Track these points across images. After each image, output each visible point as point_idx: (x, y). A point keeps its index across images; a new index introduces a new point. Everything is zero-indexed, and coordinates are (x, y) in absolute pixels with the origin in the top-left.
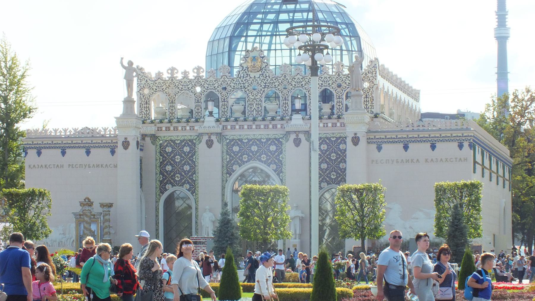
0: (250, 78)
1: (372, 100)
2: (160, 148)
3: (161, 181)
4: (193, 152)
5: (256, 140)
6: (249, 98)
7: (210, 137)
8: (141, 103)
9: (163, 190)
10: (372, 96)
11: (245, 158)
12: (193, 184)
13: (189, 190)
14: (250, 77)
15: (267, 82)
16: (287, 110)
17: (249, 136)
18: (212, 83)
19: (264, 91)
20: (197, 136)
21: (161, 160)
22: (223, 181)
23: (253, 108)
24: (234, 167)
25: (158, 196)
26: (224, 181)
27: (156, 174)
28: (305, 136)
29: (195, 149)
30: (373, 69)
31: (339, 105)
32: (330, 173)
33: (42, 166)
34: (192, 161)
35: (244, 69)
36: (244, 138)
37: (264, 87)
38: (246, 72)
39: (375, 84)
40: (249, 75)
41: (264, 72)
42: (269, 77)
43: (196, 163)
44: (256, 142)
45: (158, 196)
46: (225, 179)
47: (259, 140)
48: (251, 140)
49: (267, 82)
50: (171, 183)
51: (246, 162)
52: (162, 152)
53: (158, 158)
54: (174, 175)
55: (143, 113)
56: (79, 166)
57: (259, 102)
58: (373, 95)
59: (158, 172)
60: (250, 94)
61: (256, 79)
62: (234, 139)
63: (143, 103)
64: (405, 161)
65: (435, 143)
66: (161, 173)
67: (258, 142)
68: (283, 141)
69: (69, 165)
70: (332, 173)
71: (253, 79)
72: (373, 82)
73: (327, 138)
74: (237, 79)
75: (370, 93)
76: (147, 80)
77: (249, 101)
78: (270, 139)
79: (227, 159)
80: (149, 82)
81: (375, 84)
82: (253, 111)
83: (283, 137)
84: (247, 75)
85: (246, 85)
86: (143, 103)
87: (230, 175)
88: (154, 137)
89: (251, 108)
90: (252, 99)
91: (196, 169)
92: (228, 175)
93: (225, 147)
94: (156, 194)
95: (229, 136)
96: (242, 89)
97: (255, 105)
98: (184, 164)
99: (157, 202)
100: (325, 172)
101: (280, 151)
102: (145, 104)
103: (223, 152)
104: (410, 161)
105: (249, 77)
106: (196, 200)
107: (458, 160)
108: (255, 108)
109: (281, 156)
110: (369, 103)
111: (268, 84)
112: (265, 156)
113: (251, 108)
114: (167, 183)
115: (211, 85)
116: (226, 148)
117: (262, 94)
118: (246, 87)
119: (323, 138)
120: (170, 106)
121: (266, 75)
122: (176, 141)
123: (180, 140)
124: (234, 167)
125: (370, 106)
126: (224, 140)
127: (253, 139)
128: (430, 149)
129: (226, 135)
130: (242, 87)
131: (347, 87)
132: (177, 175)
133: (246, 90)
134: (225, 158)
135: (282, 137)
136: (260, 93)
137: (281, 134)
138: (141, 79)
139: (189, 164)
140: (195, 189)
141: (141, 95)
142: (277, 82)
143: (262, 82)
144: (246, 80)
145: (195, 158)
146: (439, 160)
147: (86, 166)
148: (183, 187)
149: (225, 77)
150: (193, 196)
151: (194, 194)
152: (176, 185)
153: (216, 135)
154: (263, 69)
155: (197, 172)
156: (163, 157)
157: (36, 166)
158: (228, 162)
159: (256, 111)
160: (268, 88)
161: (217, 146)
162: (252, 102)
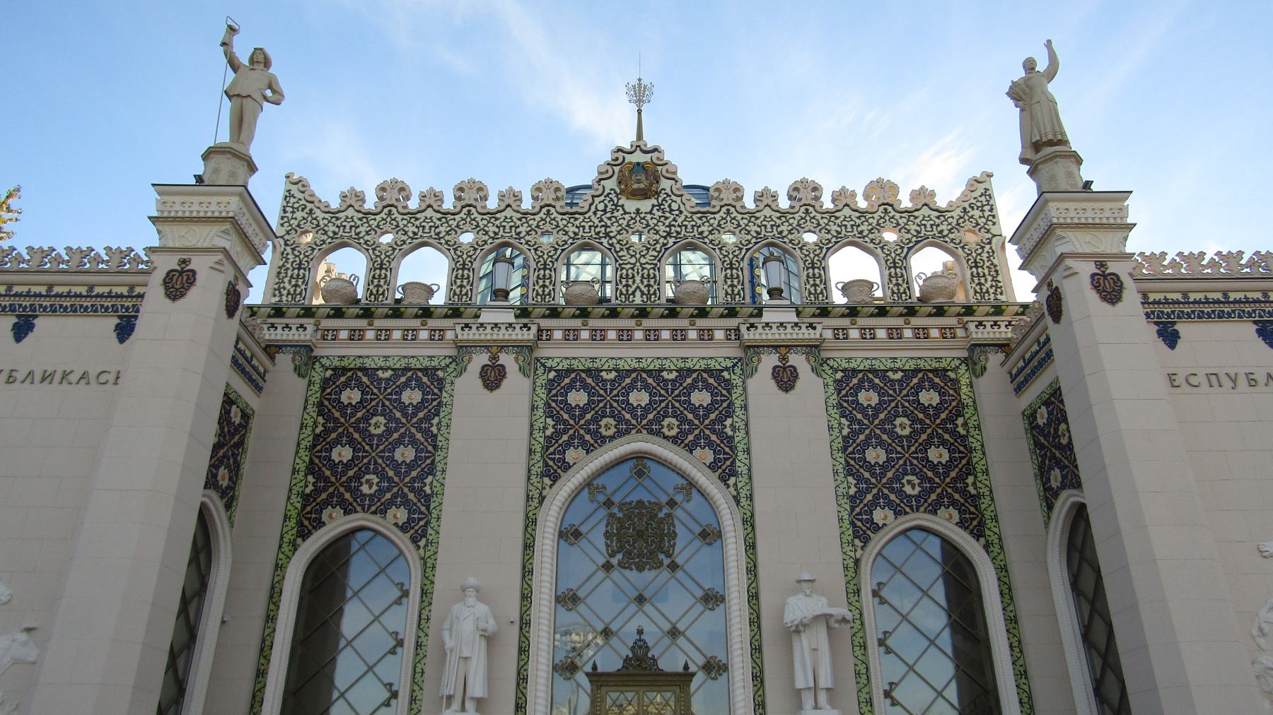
0: (626, 213)
2: (323, 392)
4: (433, 405)
5: (644, 375)
6: (621, 262)
7: (494, 358)
8: (283, 265)
9: (307, 524)
10: (992, 264)
11: (607, 427)
12: (423, 509)
13: (403, 528)
14: (623, 209)
15: (673, 223)
20: (450, 357)
23: (634, 287)
24: (571, 455)
25: (286, 548)
26: (535, 500)
27: (295, 471)
28: (808, 359)
29: (440, 397)
30: (983, 199)
31: (898, 285)
34: (427, 433)
35: (605, 194)
36: (606, 367)
39: (995, 236)
40: (622, 206)
41: (664, 199)
43: (439, 438)
44: (644, 380)
45: (286, 548)
47: (656, 374)
48: (629, 372)
49: (673, 223)
51: (612, 438)
52: (327, 406)
53: (310, 422)
54: (358, 477)
55: (285, 292)
57: (652, 271)
58: (995, 262)
59: (302, 467)
60: (624, 253)
61: (642, 216)
66: (311, 469)
67: (650, 381)
68: (733, 377)
70: (907, 478)
71: (634, 216)
72: (988, 231)
74: (587, 216)
75: (985, 255)
77: (622, 269)
79: (545, 428)
81: (995, 236)
82: (633, 293)
83: (734, 366)
84: (616, 205)
85: (614, 229)
86: (289, 266)
87: (555, 478)
89: (627, 286)
90: (629, 263)
91: (437, 459)
92: (547, 480)
93: (542, 393)
94: (282, 538)
95: (556, 360)
97: (638, 279)
98: (399, 442)
99: (279, 568)
101: (723, 406)
102: (294, 269)
103: (533, 408)
105: (621, 211)
106: (425, 563)
108: (638, 287)
109: (728, 422)
110: (986, 280)
111: (679, 229)
112: (674, 421)
114: (326, 503)
116: (544, 396)
117: (659, 252)
118: (611, 234)
119: (861, 371)
120: (374, 277)
121: (670, 206)
122: (380, 373)
123: (392, 370)
124: (571, 455)
125: (992, 286)
126: (540, 371)
127: (635, 370)
129: (548, 359)
130: (601, 235)
132: (367, 477)
133: (614, 241)
134: (538, 425)
135: (730, 365)
136: (654, 249)
137: (725, 358)
139: (414, 442)
141: (286, 245)
144: (614, 219)
145: (440, 422)
148: (385, 518)
150: (418, 547)
153: (517, 353)
154: (660, 192)
155: (439, 467)
158: (548, 439)
159: (643, 293)
161: (517, 385)
162: (630, 271)
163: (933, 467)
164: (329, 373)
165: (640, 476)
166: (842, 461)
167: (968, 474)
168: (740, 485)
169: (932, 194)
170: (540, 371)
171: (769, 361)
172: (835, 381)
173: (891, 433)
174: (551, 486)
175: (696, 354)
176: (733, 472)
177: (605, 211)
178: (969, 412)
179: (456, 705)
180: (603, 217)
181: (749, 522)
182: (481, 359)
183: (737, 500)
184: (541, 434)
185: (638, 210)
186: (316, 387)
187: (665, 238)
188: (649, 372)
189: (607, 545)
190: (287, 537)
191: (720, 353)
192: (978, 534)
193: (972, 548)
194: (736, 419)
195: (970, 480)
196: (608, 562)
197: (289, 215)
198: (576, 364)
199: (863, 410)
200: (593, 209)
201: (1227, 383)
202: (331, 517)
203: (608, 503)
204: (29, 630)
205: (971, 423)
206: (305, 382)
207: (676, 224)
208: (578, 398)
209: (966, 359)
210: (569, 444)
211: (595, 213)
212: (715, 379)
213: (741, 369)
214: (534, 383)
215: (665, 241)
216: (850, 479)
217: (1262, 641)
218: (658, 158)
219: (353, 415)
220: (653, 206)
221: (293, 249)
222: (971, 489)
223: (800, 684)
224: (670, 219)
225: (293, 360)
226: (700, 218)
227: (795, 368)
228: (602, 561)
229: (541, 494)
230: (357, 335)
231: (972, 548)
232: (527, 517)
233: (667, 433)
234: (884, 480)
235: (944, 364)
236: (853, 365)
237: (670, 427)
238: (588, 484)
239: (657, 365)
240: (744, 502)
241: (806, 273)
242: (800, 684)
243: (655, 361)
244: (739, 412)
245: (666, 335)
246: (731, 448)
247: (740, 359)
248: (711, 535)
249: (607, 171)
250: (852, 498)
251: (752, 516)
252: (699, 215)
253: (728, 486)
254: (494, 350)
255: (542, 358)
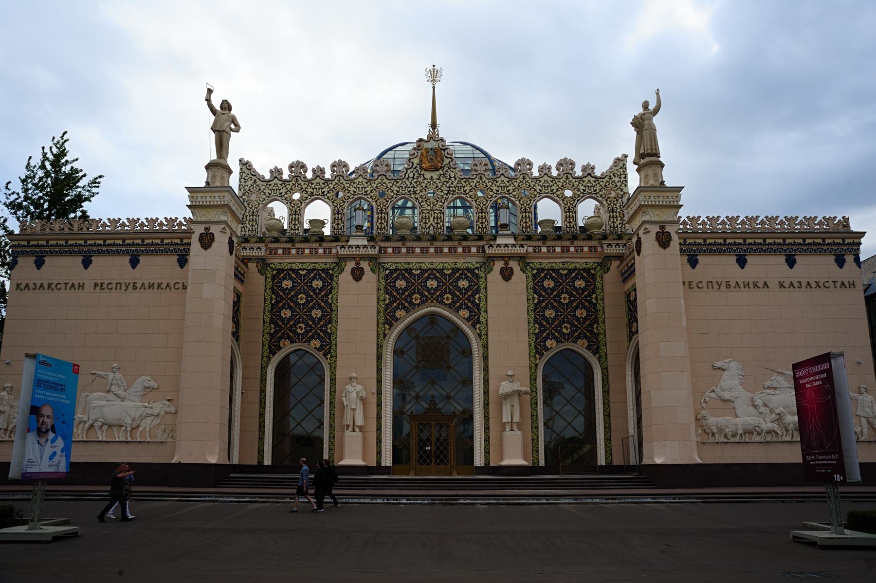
0: (425, 179)
1: (622, 216)
2: (273, 282)
3: (273, 334)
4: (329, 288)
5: (435, 272)
6: (422, 209)
7: (358, 264)
10: (622, 210)
12: (328, 340)
13: (319, 350)
14: (424, 177)
15: (451, 185)
16: (486, 227)
17: (423, 265)
18: (363, 186)
19: (446, 199)
20: (335, 263)
21: (273, 301)
22: (378, 335)
23: (429, 224)
26: (381, 337)
28: (519, 265)
29: (331, 284)
30: (621, 170)
31: (570, 222)
32: (560, 325)
33: (42, 285)
34: (326, 302)
35: (414, 167)
36: (415, 268)
37: (446, 192)
38: (417, 171)
40: (423, 175)
41: (447, 171)
42: (455, 179)
43: (333, 305)
44: (434, 275)
46: (382, 333)
47: (441, 271)
48: (427, 270)
49: (451, 185)
50: (289, 337)
52: (276, 289)
53: (269, 298)
54: (295, 325)
56: (114, 286)
57: (439, 214)
59: (268, 320)
60: (424, 203)
61: (434, 181)
62: (398, 270)
63: (247, 214)
64: (741, 285)
65: (795, 255)
66: (272, 321)
67: (438, 275)
68: (480, 272)
69: (96, 285)
70: (564, 325)
71: (429, 181)
72: (622, 190)
73: (553, 270)
74: (404, 181)
75: (618, 205)
76: (255, 180)
77: (423, 213)
78: (458, 269)
79: (385, 300)
80: (259, 182)
81: (625, 193)
82: (429, 227)
83: (480, 267)
84: (420, 175)
85: (418, 189)
86: (247, 214)
87: (391, 325)
88: (263, 264)
89: (426, 223)
91: (333, 316)
92: (387, 326)
93: (383, 281)
96: (410, 194)
97: (431, 219)
98: (313, 307)
100: (552, 323)
101: (475, 288)
102: (250, 216)
103: (379, 290)
104: (751, 285)
105: (422, 178)
106: (331, 366)
107: (838, 284)
108: (431, 224)
109: (477, 296)
110: (617, 220)
111: (454, 189)
112: (449, 296)
113: (426, 223)
114: (281, 338)
115: (360, 188)
116: (384, 283)
117: (444, 203)
118: (417, 192)
120: (292, 219)
121: (450, 175)
122: (300, 272)
123: (307, 270)
125: (620, 224)
126: (381, 270)
127: (429, 269)
128: (786, 266)
129: (385, 263)
130: (411, 192)
131: (582, 195)
132: (299, 325)
134: (382, 298)
135: (479, 266)
136: (441, 201)
137: (476, 263)
138: (247, 178)
139: (320, 307)
140: (330, 347)
142: (469, 185)
143: (444, 186)
144: (418, 183)
145: (332, 298)
146: (804, 284)
147: (127, 287)
149: (384, 177)
150: (327, 359)
151: (329, 356)
152: (297, 340)
153: (369, 261)
154: (445, 166)
155: (334, 320)
156: (278, 296)
157: (31, 286)
158: (387, 305)
159: (434, 228)
160: (453, 194)
162: (427, 214)
163: (578, 319)
164: (275, 272)
165: (433, 324)
166: (533, 316)
167: (594, 323)
168: (481, 328)
169: (593, 168)
170: (381, 270)
171: (499, 265)
172: (533, 275)
173: (559, 302)
174: (389, 329)
175: (462, 262)
176: (479, 322)
177: (413, 178)
178: (599, 291)
179: (351, 429)
180: (412, 182)
181: (486, 347)
182: (351, 265)
183: (480, 335)
185: (432, 177)
186: (270, 280)
187: (447, 194)
188: (437, 270)
190: (265, 354)
191: (473, 261)
192: (595, 352)
193: (594, 361)
194: (481, 295)
195: (595, 326)
197: (244, 184)
198: (399, 266)
199: (545, 290)
200: (407, 177)
201: (716, 286)
202: (284, 344)
203: (417, 337)
204: (169, 400)
205: (599, 297)
206: (263, 278)
207: (453, 186)
208: (401, 284)
209: (601, 263)
210: (397, 308)
211: (408, 179)
212: (470, 274)
214: (379, 276)
215: (447, 197)
216: (536, 325)
217: (704, 405)
218: (442, 145)
219: (289, 294)
220: (440, 175)
221: (248, 204)
222: (595, 330)
223: (505, 420)
224: (450, 183)
225: (257, 266)
226: (465, 182)
227: (512, 268)
228: (414, 364)
229: (384, 333)
230: (287, 252)
231: (594, 361)
232: (378, 344)
233: (446, 302)
234: (553, 326)
235: (589, 266)
236: (543, 266)
237: (448, 299)
238: (408, 328)
239: (441, 266)
241: (521, 215)
242: (505, 420)
244: (482, 291)
245: (446, 250)
246: (478, 310)
247: (484, 263)
248: (467, 353)
249: (414, 154)
250: (536, 335)
251: (487, 344)
252: (464, 180)
254: (357, 259)
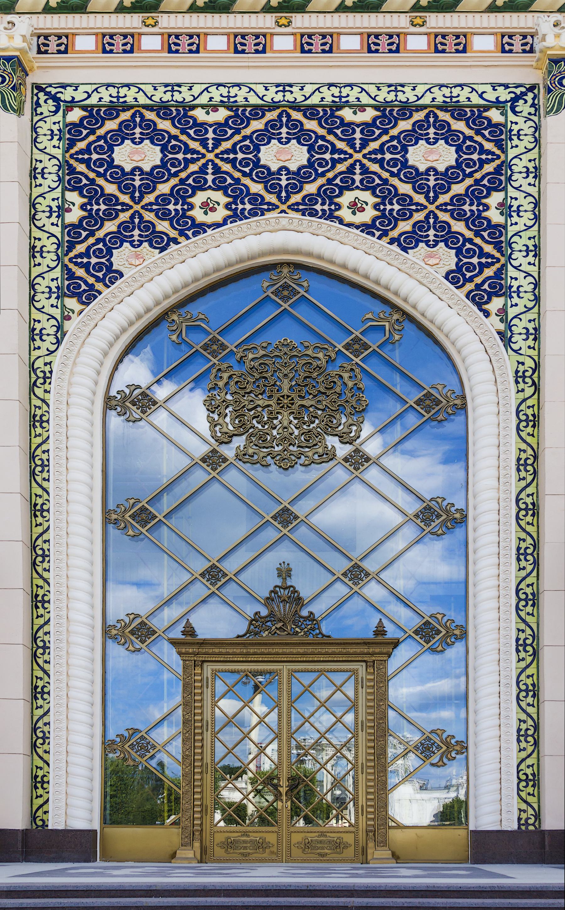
11: (207, 207)
36: (204, 99)
46: (49, 327)
62: (127, 107)
68: (511, 117)
79: (62, 210)
83: (516, 99)
95: (81, 88)
116: (58, 153)
127: (273, 106)
168: (512, 312)
184: (54, 219)
189: (213, 424)
194: (512, 192)
196: (214, 451)
198: (130, 95)
213: (533, 105)
228: (202, 449)
229: (59, 327)
232: (33, 368)
237: (355, 207)
239: (328, 95)
240: (519, 341)
243: (324, 89)
246: (498, 246)
253: (487, 314)
255: (50, 85)
